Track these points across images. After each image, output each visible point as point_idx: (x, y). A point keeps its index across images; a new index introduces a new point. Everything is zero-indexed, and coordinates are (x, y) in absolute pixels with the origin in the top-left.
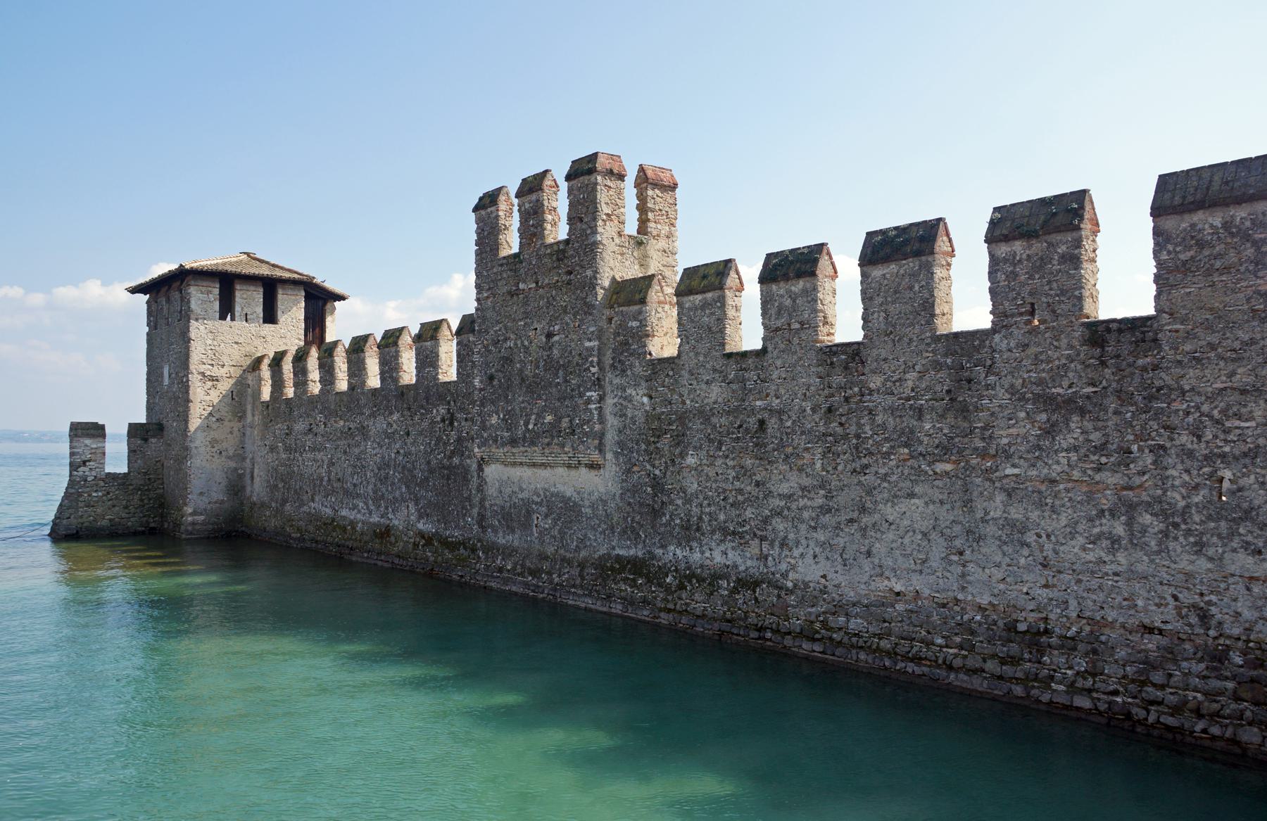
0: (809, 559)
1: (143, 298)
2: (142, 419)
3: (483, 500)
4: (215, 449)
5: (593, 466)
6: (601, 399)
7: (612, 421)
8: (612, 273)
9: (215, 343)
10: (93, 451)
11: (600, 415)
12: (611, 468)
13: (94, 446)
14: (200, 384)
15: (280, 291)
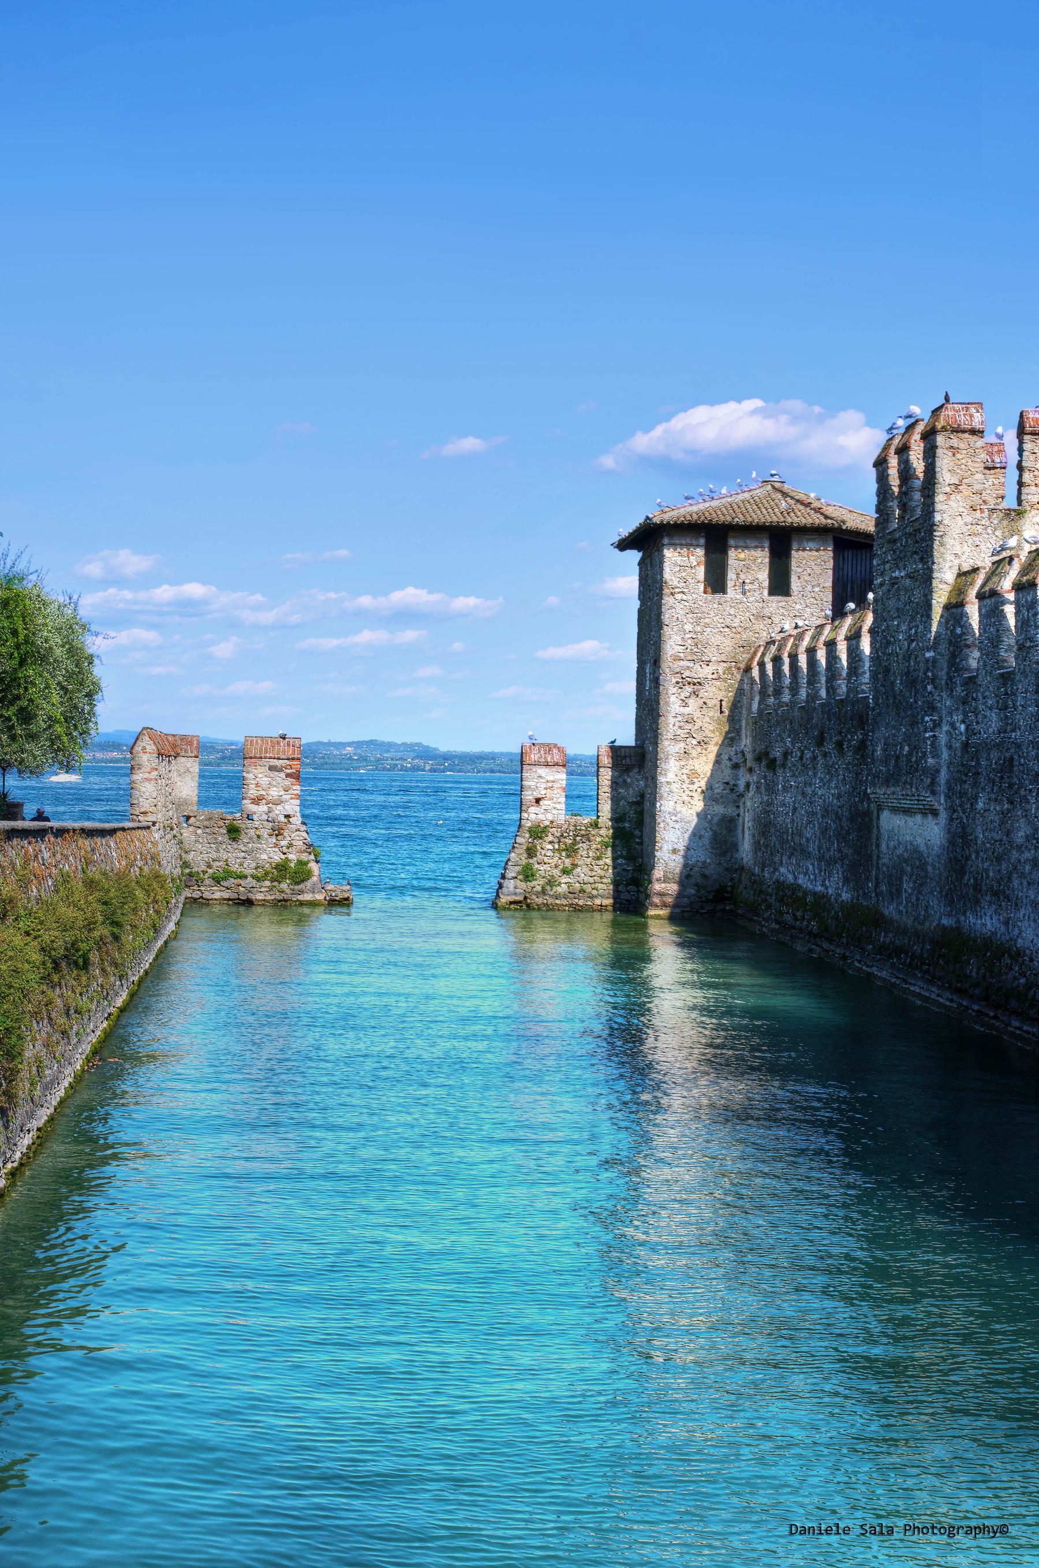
0: (1026, 923)
1: (634, 556)
2: (627, 738)
3: (878, 857)
4: (695, 787)
5: (935, 813)
6: (937, 725)
7: (945, 755)
8: (957, 562)
9: (699, 629)
10: (550, 785)
11: (933, 745)
12: (943, 815)
13: (550, 778)
14: (674, 690)
15: (795, 546)
